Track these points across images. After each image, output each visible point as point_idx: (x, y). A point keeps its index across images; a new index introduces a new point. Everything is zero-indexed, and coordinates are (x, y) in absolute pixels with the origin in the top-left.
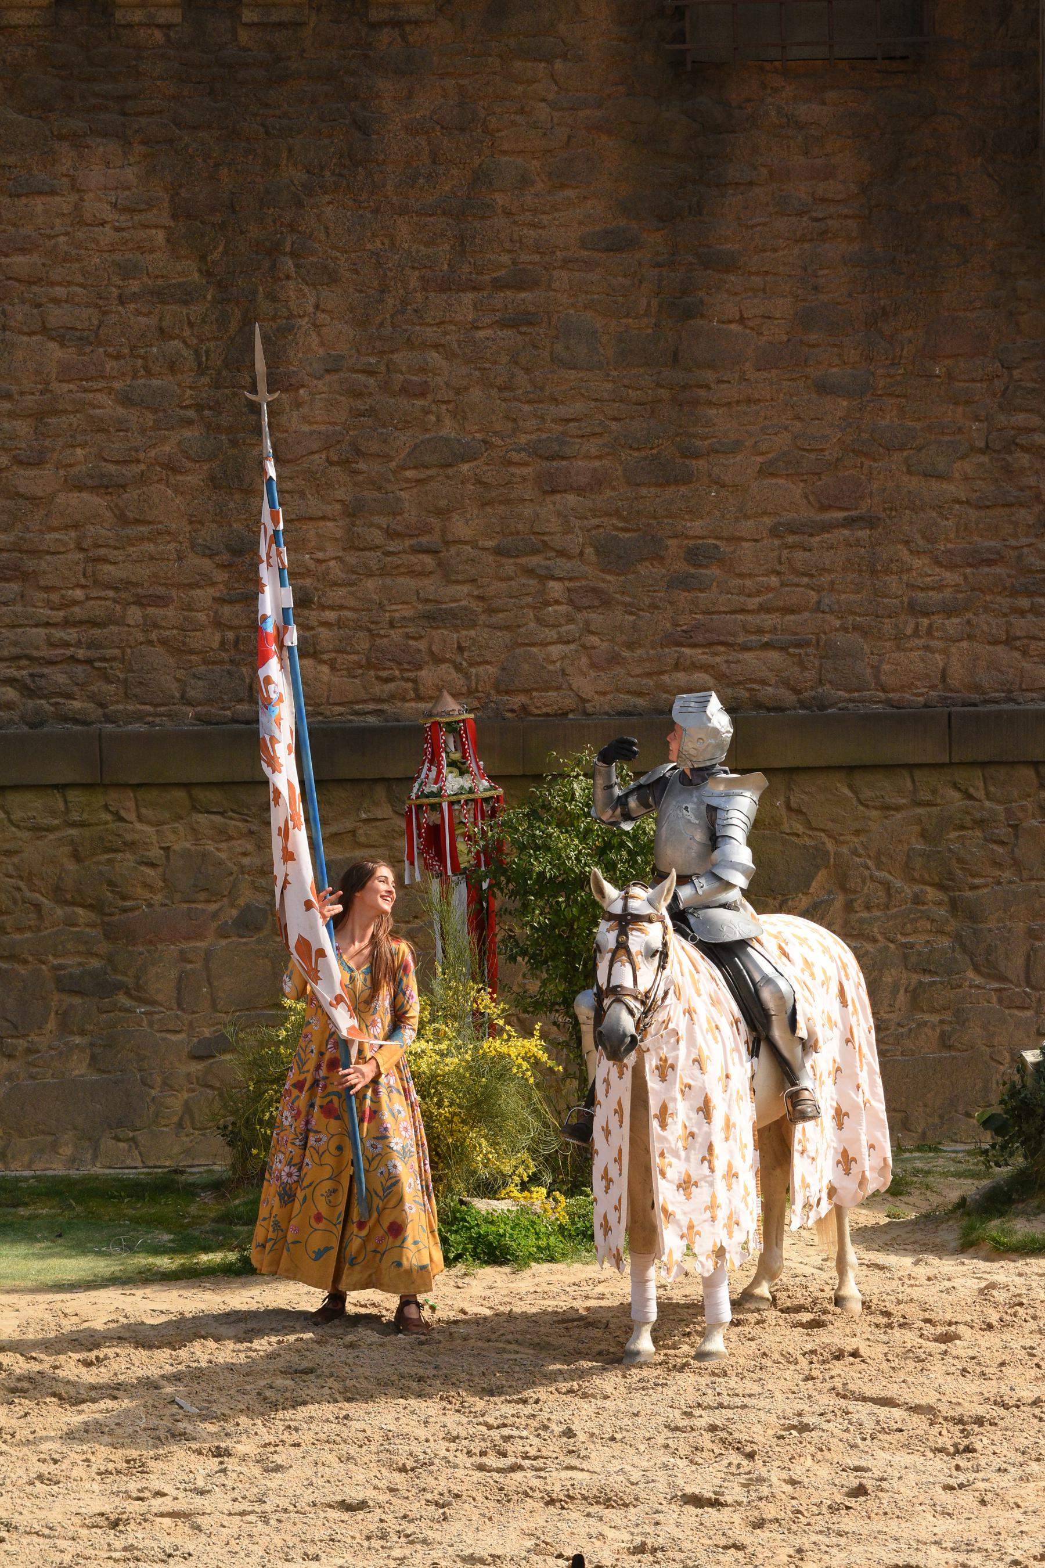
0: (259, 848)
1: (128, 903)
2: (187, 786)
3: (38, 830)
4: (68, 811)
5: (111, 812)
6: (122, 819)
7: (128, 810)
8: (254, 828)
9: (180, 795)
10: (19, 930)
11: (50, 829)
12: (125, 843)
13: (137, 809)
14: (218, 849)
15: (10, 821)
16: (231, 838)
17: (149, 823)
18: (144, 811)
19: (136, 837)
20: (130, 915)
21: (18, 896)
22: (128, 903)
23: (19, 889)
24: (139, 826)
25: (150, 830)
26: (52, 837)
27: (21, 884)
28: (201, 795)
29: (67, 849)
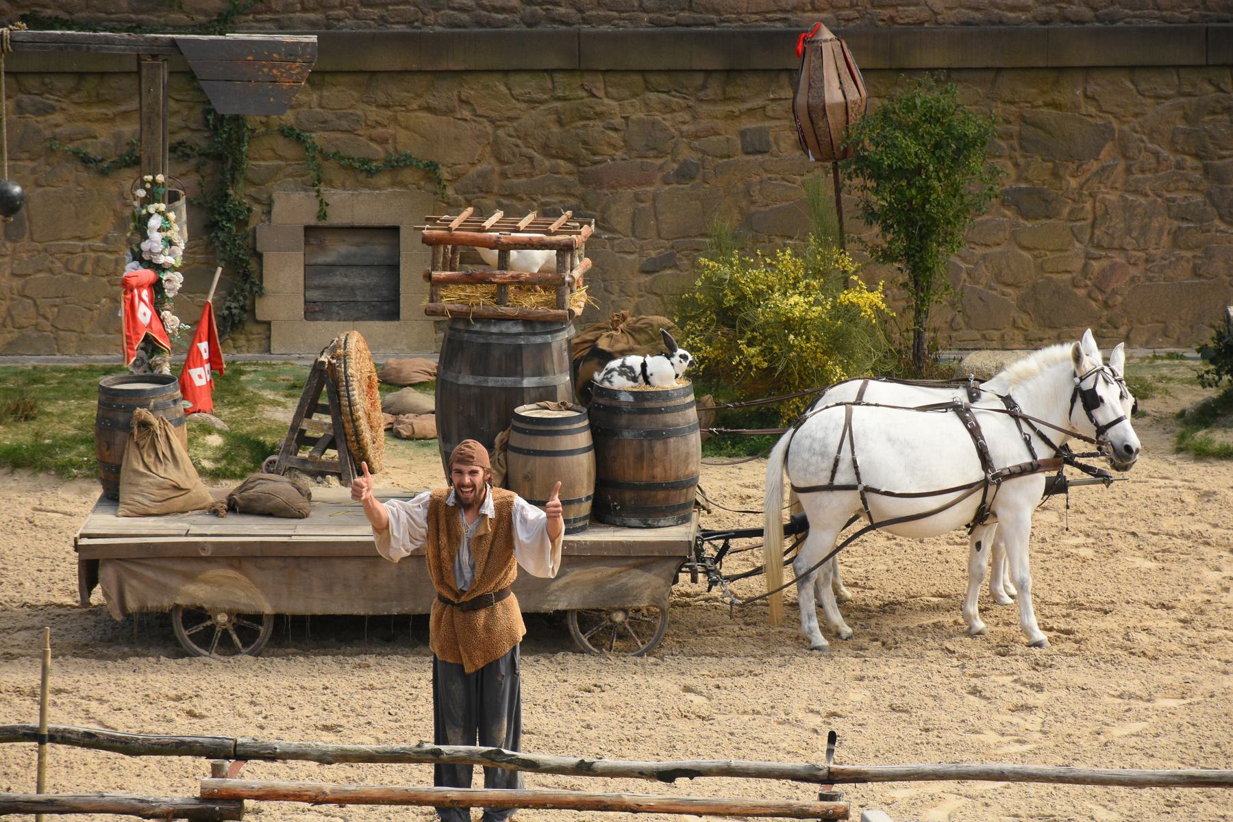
0: (694, 118)
1: (597, 158)
2: (642, 72)
3: (533, 102)
4: (554, 88)
5: (586, 90)
6: (594, 96)
7: (597, 89)
8: (691, 103)
9: (637, 78)
10: (517, 176)
11: (541, 102)
12: (596, 114)
13: (605, 88)
14: (664, 119)
15: (512, 95)
16: (674, 111)
17: (614, 99)
18: (610, 89)
19: (604, 108)
20: (599, 166)
21: (517, 150)
22: (597, 158)
23: (517, 146)
24: (606, 101)
25: (614, 103)
26: (542, 107)
27: (519, 142)
28: (653, 79)
29: (553, 117)
